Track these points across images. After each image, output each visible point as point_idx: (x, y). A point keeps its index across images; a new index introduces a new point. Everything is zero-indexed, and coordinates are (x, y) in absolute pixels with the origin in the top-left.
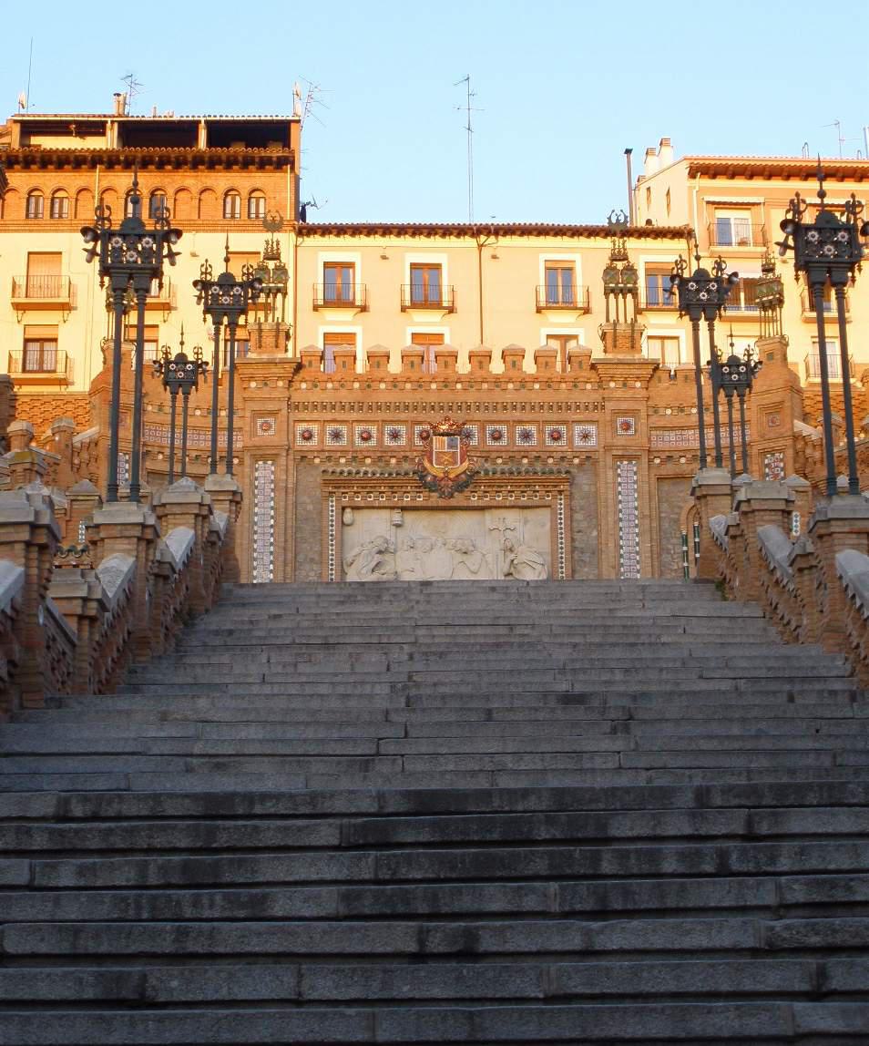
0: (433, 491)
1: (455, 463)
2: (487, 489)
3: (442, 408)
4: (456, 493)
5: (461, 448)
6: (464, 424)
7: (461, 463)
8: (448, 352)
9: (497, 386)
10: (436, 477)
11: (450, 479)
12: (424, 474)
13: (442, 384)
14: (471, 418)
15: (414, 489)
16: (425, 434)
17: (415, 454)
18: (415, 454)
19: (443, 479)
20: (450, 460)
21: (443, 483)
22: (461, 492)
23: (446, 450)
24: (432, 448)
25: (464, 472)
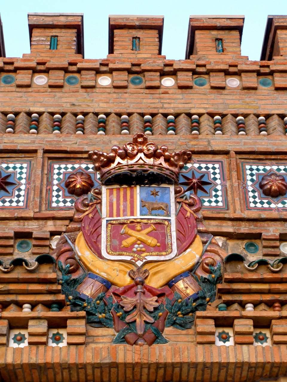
0: (100, 324)
1: (163, 247)
2: (264, 312)
3: (126, 125)
4: (168, 331)
5: (180, 213)
6: (187, 156)
7: (182, 250)
8: (139, 19)
9: (264, 84)
10: (108, 284)
11: (152, 291)
12: (74, 276)
13: (124, 76)
14: (201, 145)
15: (40, 311)
16: (79, 183)
17: (50, 226)
18: (50, 226)
19: (127, 290)
20: (152, 241)
21: (128, 301)
22: (183, 326)
23: (138, 216)
24: (97, 212)
25: (191, 271)
